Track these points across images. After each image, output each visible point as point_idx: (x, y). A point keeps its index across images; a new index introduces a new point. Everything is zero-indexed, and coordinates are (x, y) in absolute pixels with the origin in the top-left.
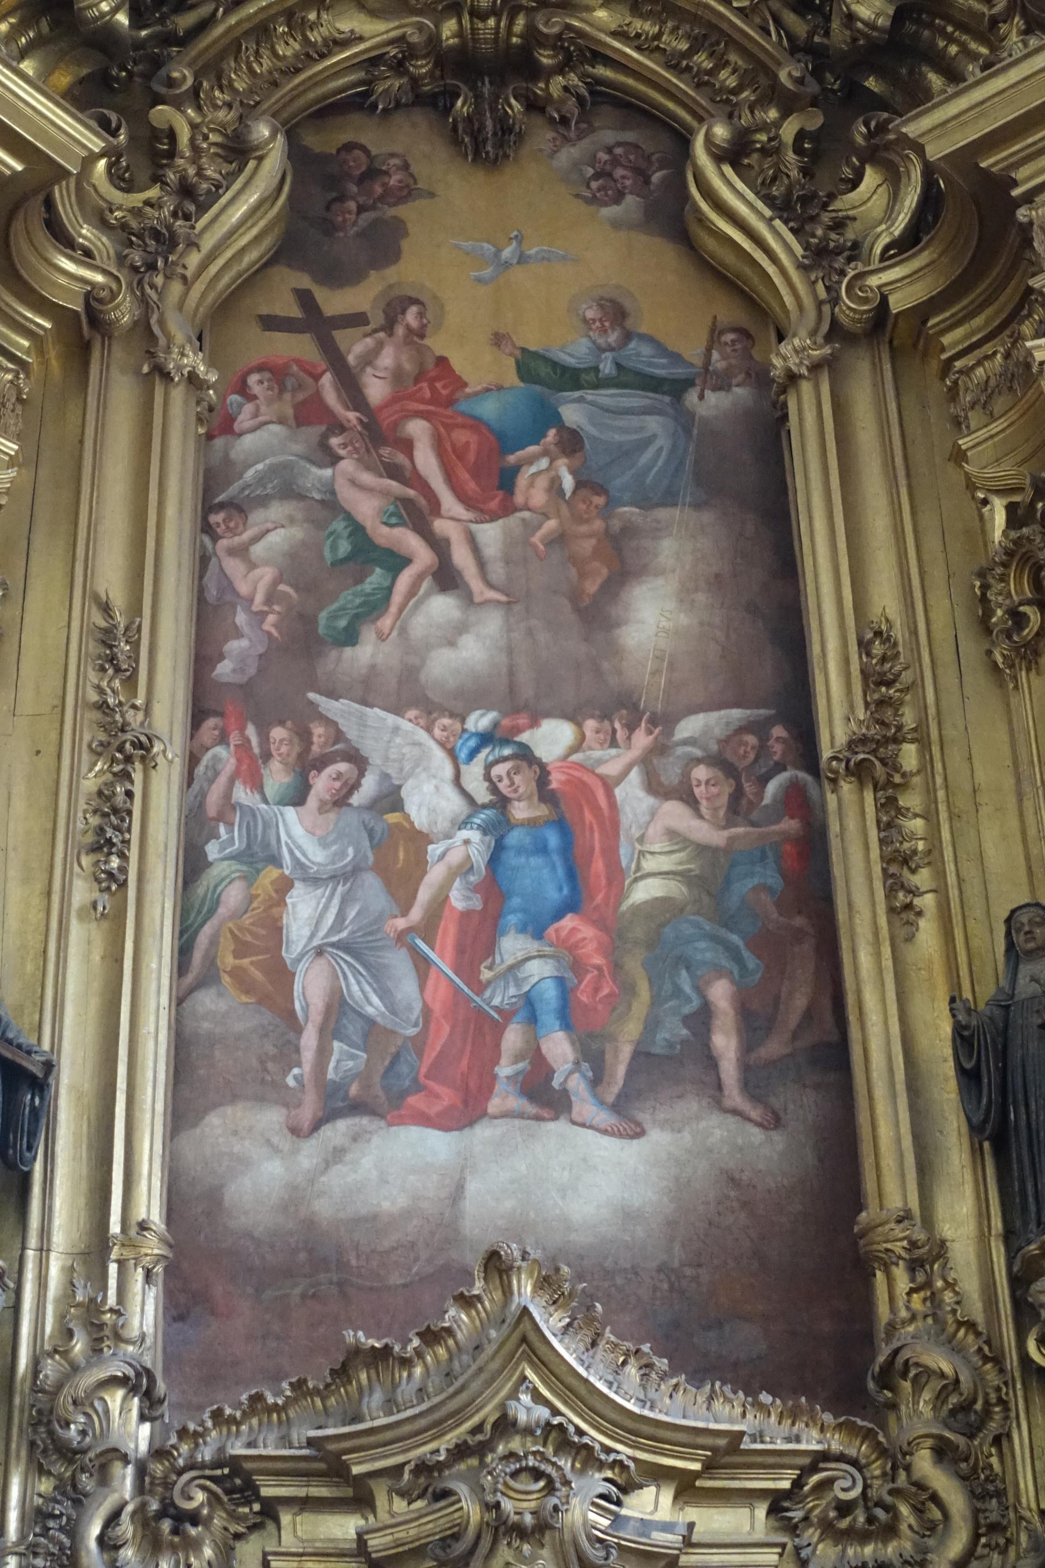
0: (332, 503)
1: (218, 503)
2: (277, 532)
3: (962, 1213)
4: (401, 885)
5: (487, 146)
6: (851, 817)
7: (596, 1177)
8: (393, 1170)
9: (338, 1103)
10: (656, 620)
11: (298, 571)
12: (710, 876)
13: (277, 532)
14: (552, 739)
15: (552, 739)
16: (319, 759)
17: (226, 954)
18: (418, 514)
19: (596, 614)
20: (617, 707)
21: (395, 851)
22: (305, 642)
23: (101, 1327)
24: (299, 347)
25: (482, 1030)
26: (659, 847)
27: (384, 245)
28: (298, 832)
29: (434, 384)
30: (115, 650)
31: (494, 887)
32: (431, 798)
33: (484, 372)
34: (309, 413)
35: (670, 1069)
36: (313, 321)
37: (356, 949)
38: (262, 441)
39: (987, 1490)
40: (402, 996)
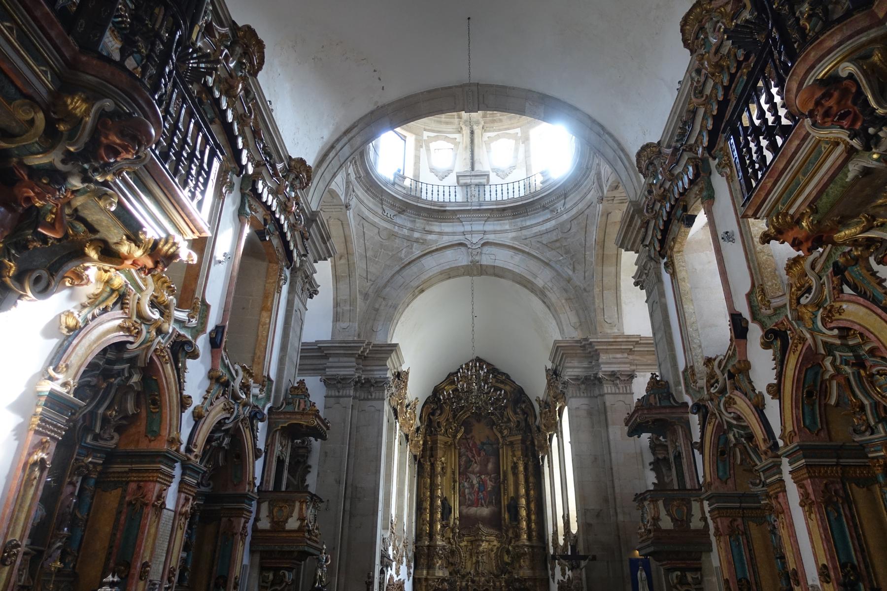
0: (468, 456)
1: (460, 456)
2: (464, 459)
3: (506, 516)
4: (473, 488)
5: (479, 421)
6: (502, 486)
7: (485, 511)
8: (473, 510)
9: (469, 506)
10: (490, 466)
11: (465, 462)
12: (493, 487)
13: (464, 459)
14: (483, 477)
15: (483, 477)
16: (468, 478)
17: (462, 495)
18: (473, 457)
19: (486, 465)
20: (487, 474)
21: (472, 486)
22: (466, 468)
23: (455, 523)
24: (464, 441)
25: (478, 500)
26: (490, 485)
27: (471, 431)
28: (466, 484)
29: (475, 444)
30: (454, 473)
31: (479, 489)
32: (475, 482)
33: (478, 443)
34: (466, 447)
35: (490, 503)
36: (466, 439)
37: (470, 494)
38: (463, 450)
39: (507, 535)
40: (473, 497)
